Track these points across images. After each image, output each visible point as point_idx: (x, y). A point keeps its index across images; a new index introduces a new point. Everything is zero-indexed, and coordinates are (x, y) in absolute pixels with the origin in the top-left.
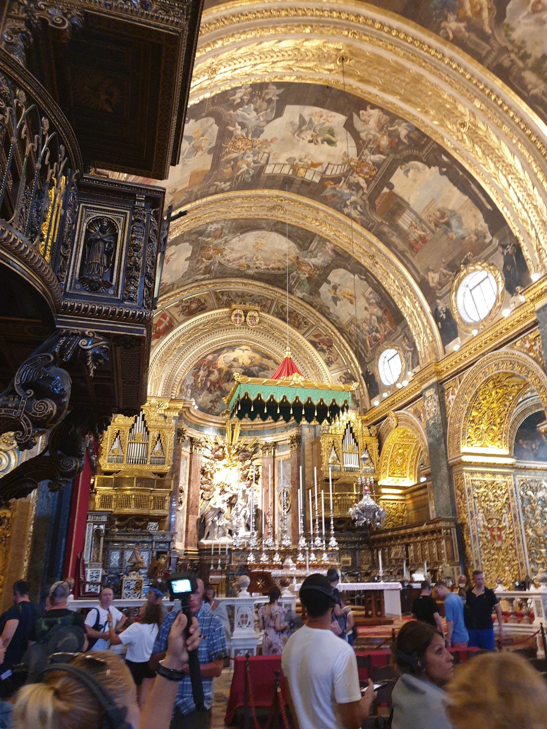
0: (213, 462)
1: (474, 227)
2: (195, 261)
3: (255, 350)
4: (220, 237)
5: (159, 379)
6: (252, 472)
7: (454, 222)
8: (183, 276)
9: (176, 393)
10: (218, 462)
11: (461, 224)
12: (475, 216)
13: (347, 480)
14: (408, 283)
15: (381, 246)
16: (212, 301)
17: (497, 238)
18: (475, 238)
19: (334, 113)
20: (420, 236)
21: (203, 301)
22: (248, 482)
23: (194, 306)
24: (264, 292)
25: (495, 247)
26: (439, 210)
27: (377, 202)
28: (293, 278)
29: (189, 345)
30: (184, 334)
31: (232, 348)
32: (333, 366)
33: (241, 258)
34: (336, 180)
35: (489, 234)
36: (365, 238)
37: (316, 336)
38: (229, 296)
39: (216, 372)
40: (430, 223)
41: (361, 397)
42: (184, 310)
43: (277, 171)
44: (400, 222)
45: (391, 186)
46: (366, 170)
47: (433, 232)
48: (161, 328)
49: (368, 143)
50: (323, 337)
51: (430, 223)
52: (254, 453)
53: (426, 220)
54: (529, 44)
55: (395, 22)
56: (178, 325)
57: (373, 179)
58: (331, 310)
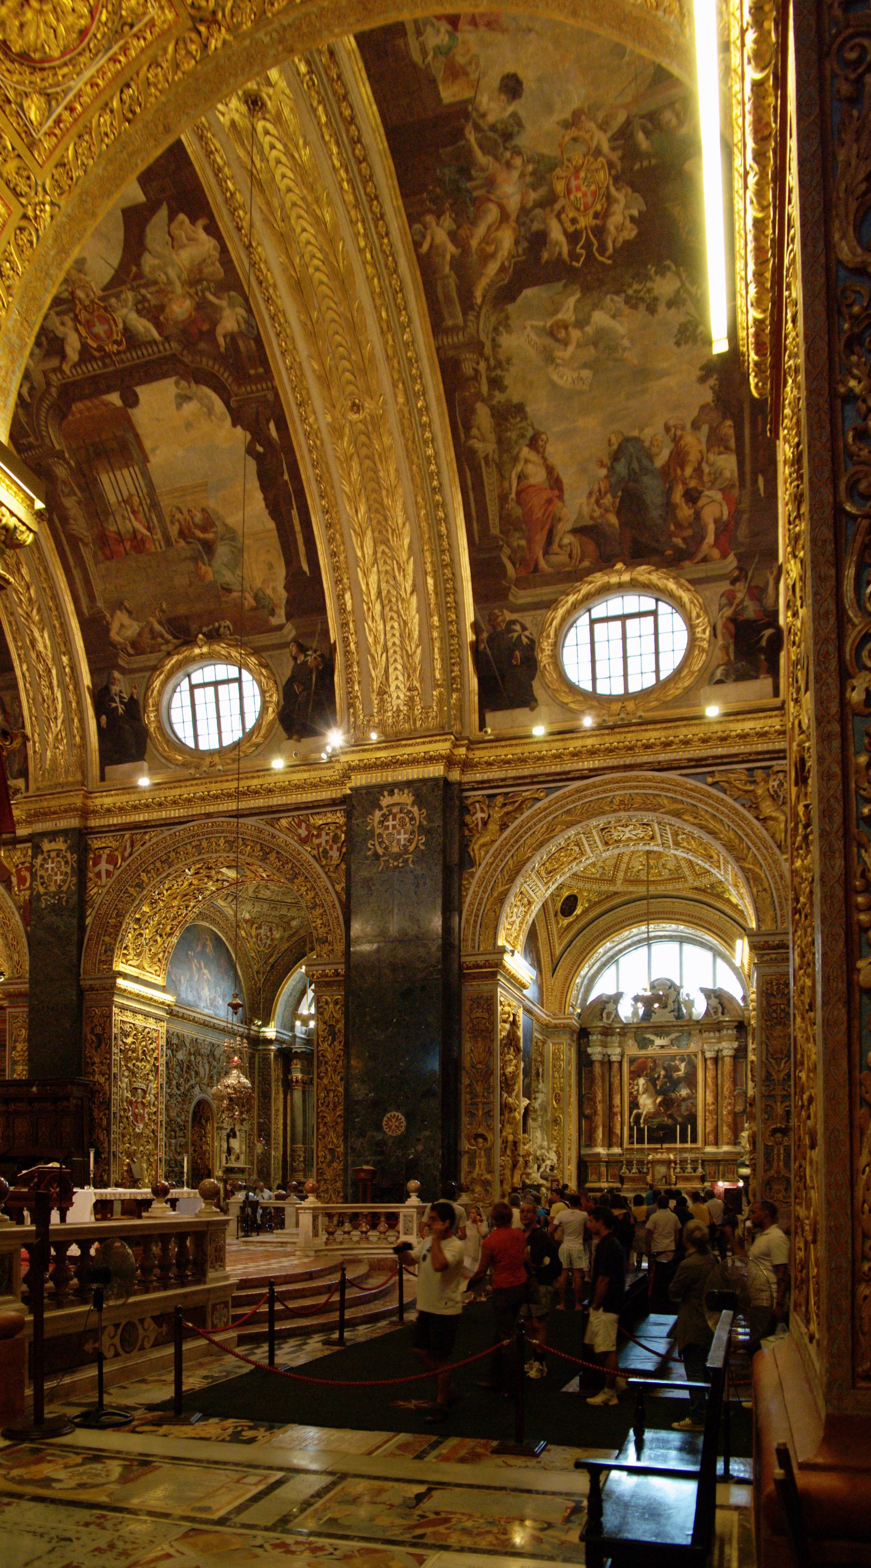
1: (258, 583)
7: (222, 551)
12: (271, 566)
17: (297, 628)
18: (254, 604)
20: (135, 531)
25: (284, 640)
26: (203, 510)
35: (282, 612)
40: (172, 523)
46: (100, 329)
47: (168, 542)
49: (146, 286)
51: (172, 523)
53: (166, 512)
57: (102, 359)
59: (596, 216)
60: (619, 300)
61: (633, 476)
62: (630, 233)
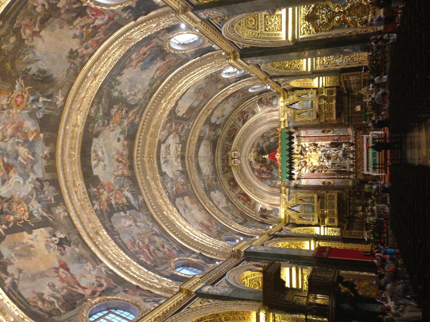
0: (308, 167)
2: (215, 188)
3: (250, 151)
4: (204, 180)
5: (271, 198)
6: (312, 148)
7: (199, 88)
8: (221, 192)
9: (276, 190)
10: (308, 164)
11: (201, 85)
13: (317, 107)
14: (221, 93)
15: (204, 109)
16: (228, 175)
19: (161, 150)
21: (229, 179)
22: (318, 149)
23: (232, 183)
24: (219, 149)
27: (188, 117)
28: (213, 137)
29: (252, 185)
30: (247, 188)
31: (251, 163)
32: (255, 110)
33: (208, 165)
34: (180, 137)
36: (201, 116)
37: (240, 121)
38: (224, 167)
39: (262, 168)
41: (270, 95)
42: (235, 188)
43: (180, 165)
44: (196, 106)
45: (183, 114)
48: (245, 198)
50: (240, 116)
52: (302, 146)
54: (144, 92)
55: (137, 141)
56: (243, 191)
58: (227, 116)
59: (118, 112)
60: (123, 95)
61: (147, 64)
62: (115, 106)
